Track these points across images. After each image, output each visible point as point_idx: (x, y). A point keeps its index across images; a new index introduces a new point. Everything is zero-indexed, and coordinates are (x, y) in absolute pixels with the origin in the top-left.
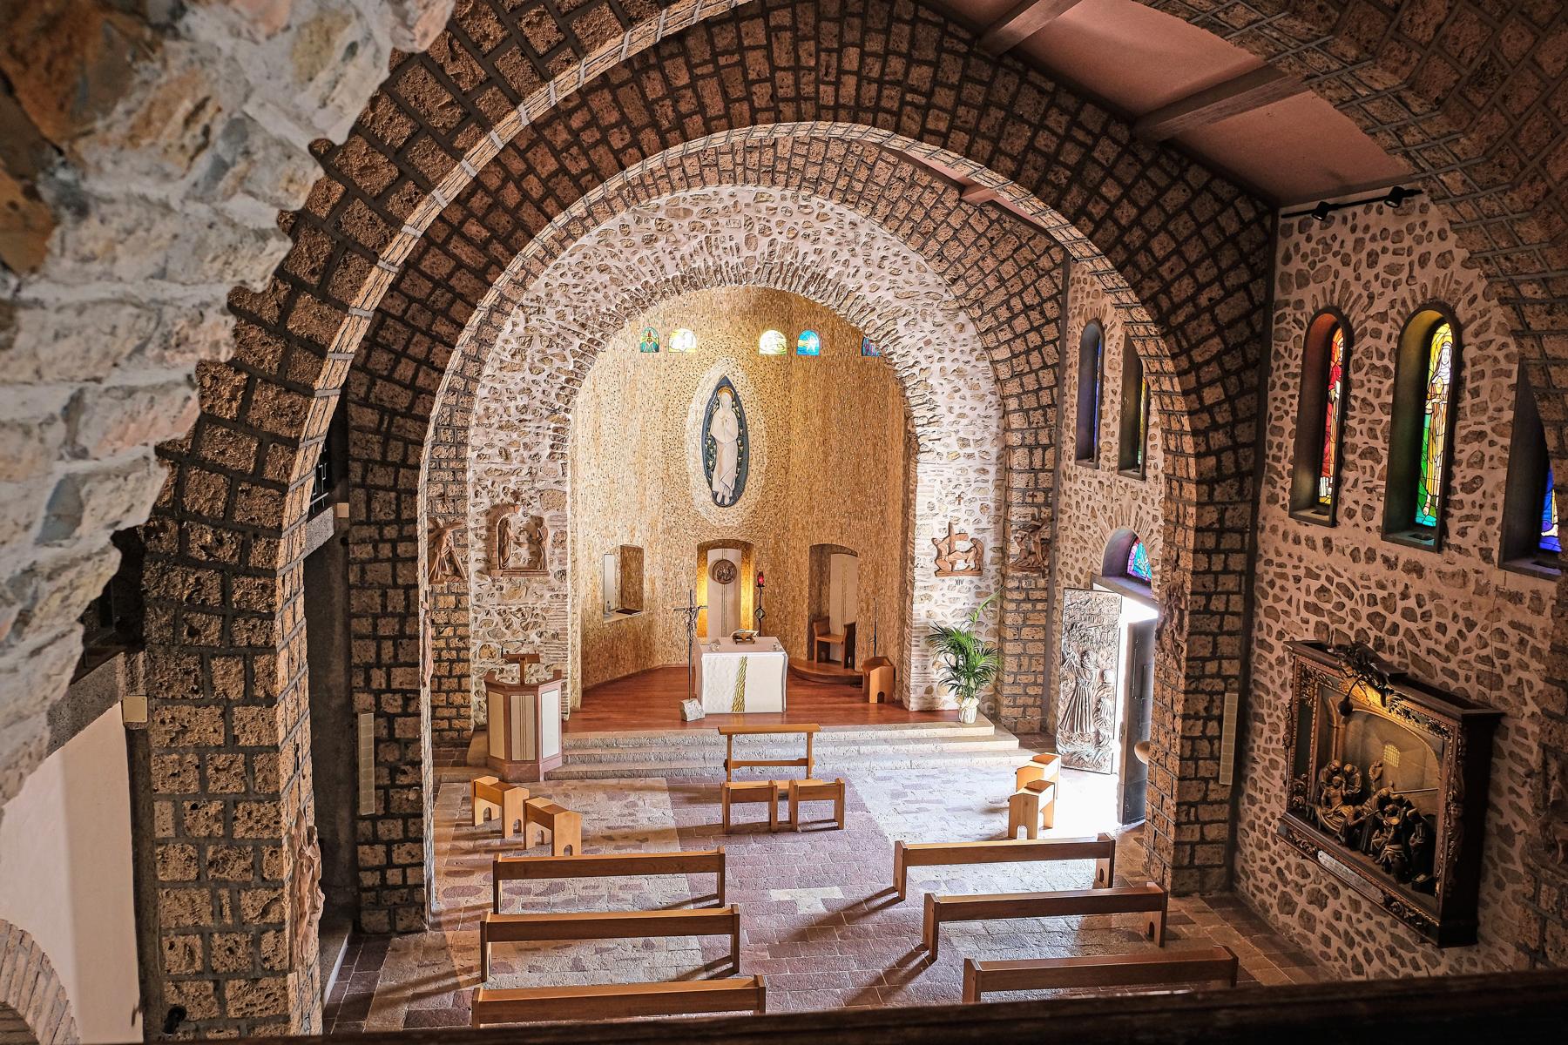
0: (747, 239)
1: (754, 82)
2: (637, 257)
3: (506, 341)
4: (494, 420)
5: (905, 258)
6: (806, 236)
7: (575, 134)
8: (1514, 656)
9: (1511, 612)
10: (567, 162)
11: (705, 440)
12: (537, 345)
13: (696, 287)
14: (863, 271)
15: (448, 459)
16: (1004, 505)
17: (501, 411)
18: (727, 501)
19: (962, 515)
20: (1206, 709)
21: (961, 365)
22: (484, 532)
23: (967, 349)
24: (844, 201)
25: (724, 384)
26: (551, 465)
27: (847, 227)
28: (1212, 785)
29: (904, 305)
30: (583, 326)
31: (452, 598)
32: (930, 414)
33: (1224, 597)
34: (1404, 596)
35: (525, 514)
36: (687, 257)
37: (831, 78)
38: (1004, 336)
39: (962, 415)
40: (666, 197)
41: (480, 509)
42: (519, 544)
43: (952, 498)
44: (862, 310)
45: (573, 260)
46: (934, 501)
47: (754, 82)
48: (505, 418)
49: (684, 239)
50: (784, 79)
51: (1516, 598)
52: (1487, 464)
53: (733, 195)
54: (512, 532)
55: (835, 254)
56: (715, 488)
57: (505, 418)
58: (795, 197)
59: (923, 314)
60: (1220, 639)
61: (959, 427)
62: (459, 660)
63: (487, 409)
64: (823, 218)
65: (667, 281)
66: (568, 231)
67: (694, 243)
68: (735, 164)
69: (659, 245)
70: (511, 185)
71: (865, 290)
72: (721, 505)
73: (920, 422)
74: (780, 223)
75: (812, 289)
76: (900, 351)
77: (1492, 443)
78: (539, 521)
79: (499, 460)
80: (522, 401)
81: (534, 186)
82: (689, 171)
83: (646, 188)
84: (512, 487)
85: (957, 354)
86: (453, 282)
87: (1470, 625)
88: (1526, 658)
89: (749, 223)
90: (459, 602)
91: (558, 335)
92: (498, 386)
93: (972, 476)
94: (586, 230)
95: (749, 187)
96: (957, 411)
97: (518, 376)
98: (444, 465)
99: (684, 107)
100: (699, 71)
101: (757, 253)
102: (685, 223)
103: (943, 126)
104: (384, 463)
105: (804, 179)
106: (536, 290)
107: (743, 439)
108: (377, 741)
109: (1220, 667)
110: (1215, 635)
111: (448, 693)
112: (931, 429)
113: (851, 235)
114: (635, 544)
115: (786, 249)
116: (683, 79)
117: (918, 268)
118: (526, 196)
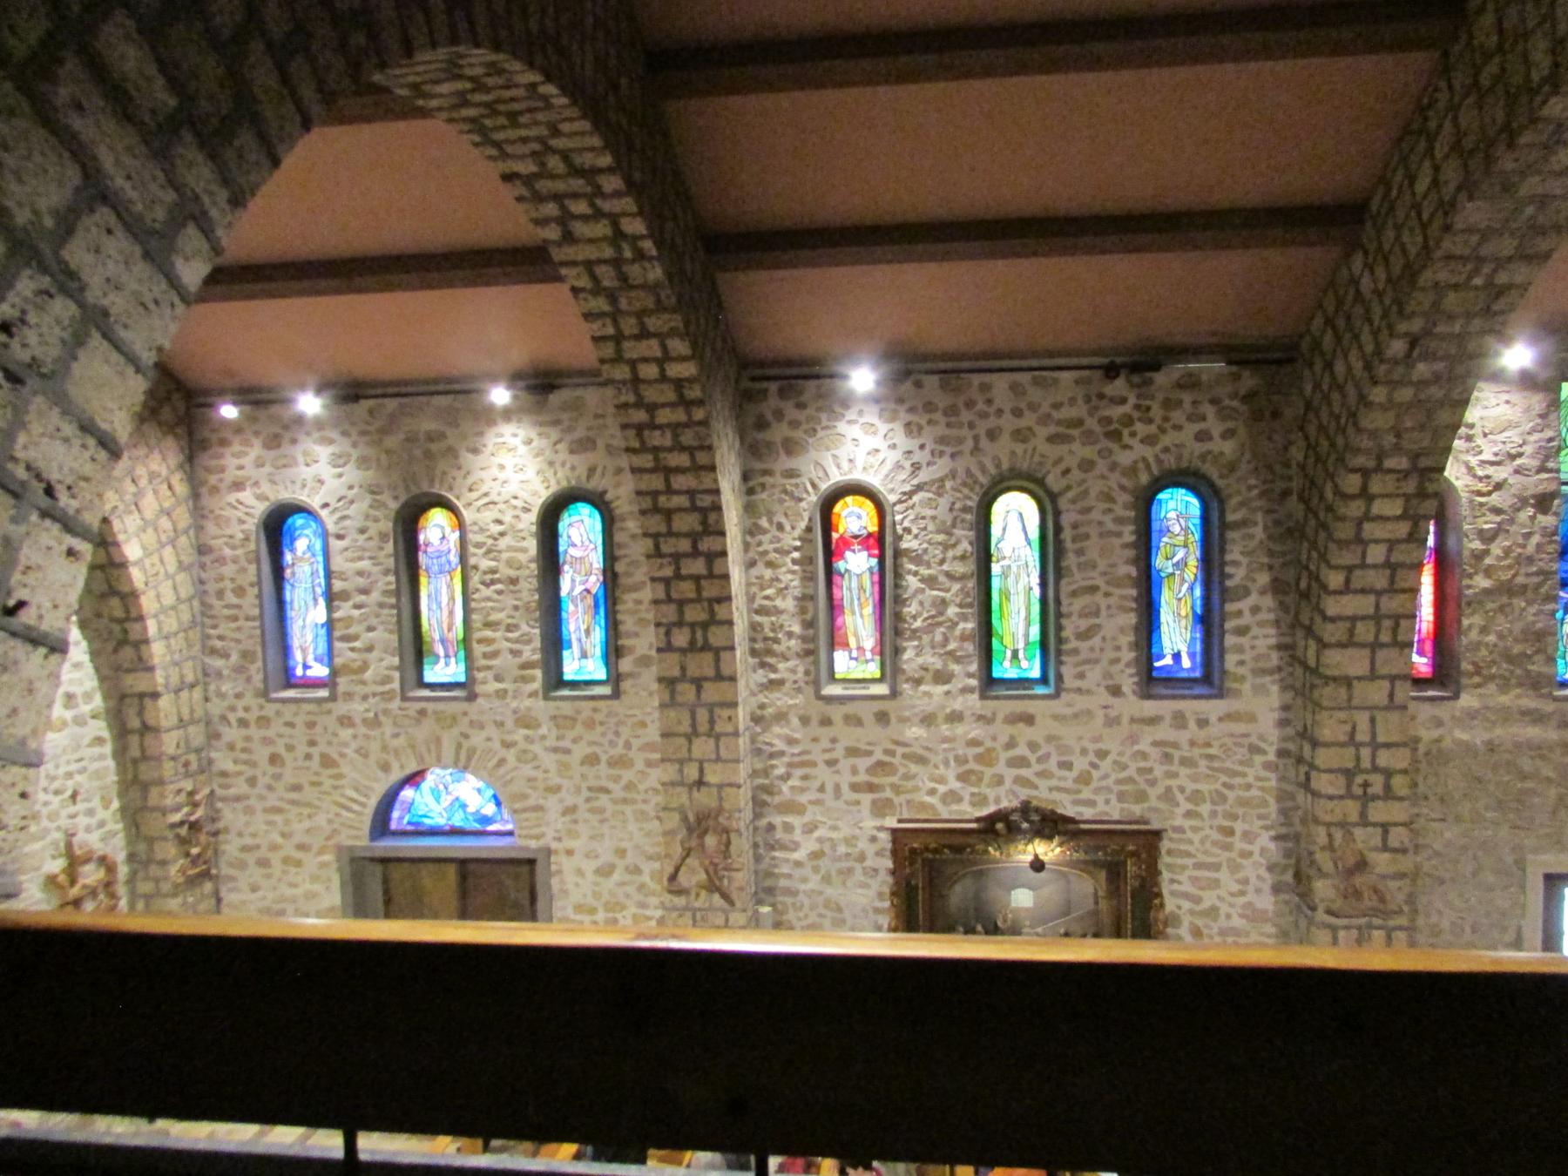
8: (1159, 771)
9: (1148, 736)
34: (1011, 744)
51: (1153, 721)
52: (1104, 613)
77: (1107, 595)
87: (1102, 754)
88: (1174, 768)
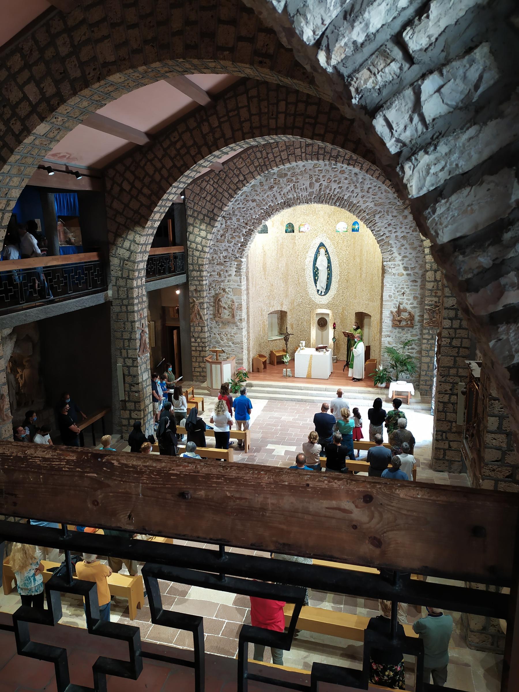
0: (310, 184)
1: (244, 122)
2: (266, 195)
3: (219, 231)
4: (215, 261)
5: (379, 187)
6: (335, 181)
7: (178, 151)
10: (176, 163)
12: (230, 232)
15: (197, 277)
16: (423, 296)
17: (218, 258)
18: (323, 294)
20: (451, 389)
21: (405, 234)
22: (212, 304)
23: (408, 227)
24: (348, 164)
25: (322, 245)
27: (353, 175)
28: (454, 424)
30: (246, 224)
31: (200, 328)
33: (460, 340)
36: (286, 193)
37: (274, 116)
40: (276, 169)
41: (212, 295)
44: (360, 212)
45: (242, 198)
46: (391, 294)
47: (244, 122)
48: (219, 260)
49: (285, 186)
50: (255, 119)
53: (304, 166)
55: (348, 188)
57: (219, 260)
58: (330, 164)
59: (388, 212)
60: (458, 359)
61: (404, 262)
62: (202, 351)
63: (213, 257)
64: (342, 172)
65: (278, 204)
66: (237, 186)
67: (289, 188)
68: (302, 153)
69: (274, 189)
70: (157, 173)
71: (361, 203)
72: (321, 295)
74: (324, 176)
75: (338, 204)
76: (377, 229)
79: (218, 277)
80: (225, 254)
81: (164, 172)
82: (283, 158)
83: (266, 166)
85: (403, 229)
86: (140, 211)
89: (311, 177)
90: (202, 329)
91: (237, 228)
92: (216, 248)
94: (244, 185)
95: (310, 161)
97: (223, 244)
98: (195, 278)
99: (217, 135)
100: (222, 120)
101: (314, 190)
102: (285, 179)
103: (322, 132)
104: (122, 278)
105: (331, 156)
106: (229, 210)
107: (329, 268)
108: (124, 375)
109: (458, 371)
110: (455, 357)
111: (199, 362)
113: (355, 179)
114: (283, 310)
115: (327, 187)
116: (216, 124)
117: (385, 191)
118: (162, 176)
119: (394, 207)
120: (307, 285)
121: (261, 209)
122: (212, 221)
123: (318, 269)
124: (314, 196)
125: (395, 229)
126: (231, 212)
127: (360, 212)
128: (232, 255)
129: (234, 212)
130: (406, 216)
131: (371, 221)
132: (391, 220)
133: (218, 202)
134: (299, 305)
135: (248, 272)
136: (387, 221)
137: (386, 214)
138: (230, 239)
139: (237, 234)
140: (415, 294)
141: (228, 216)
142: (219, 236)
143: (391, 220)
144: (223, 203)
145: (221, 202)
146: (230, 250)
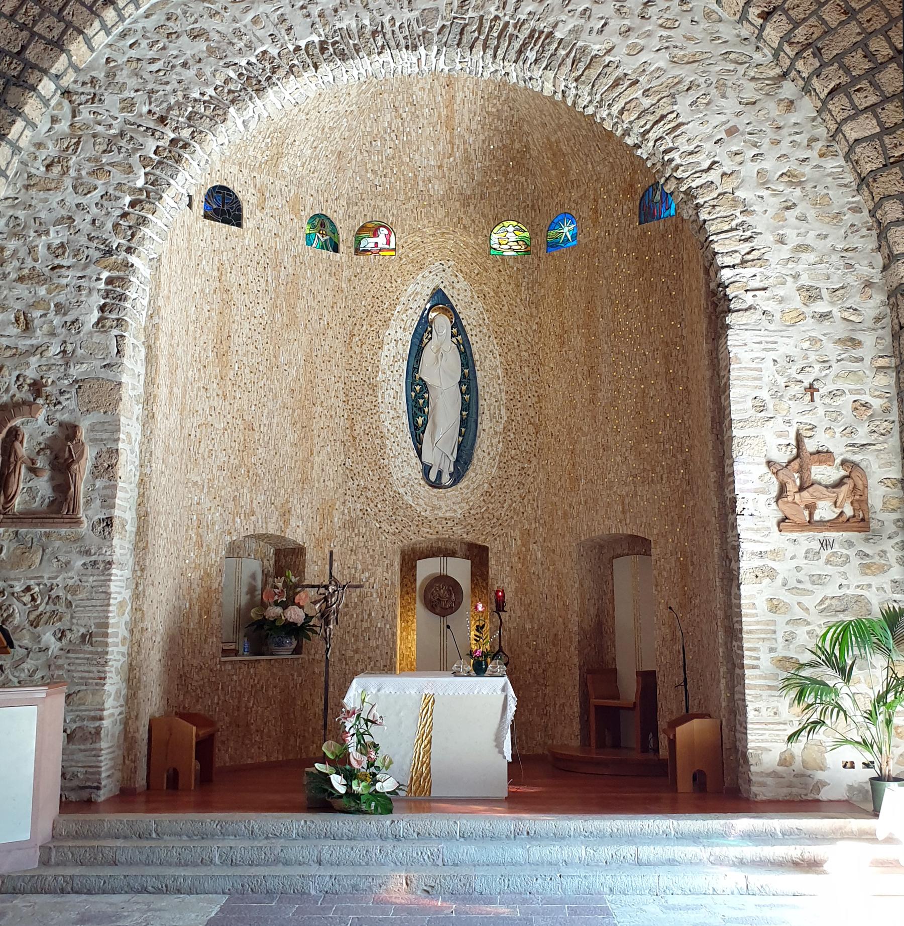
2: (251, 15)
3: (39, 145)
11: (410, 386)
12: (88, 150)
13: (343, 56)
14: (615, 24)
17: (22, 253)
19: (818, 416)
23: (802, 139)
26: (97, 338)
29: (687, 74)
30: (162, 120)
32: (745, 247)
35: (49, 421)
38: (862, 100)
39: (802, 248)
42: (33, 470)
43: (796, 389)
44: (616, 83)
45: (150, 23)
46: (765, 394)
54: (23, 449)
56: (427, 457)
57: (29, 263)
59: (721, 87)
61: (800, 267)
65: (298, 49)
72: (436, 485)
73: (728, 261)
75: (531, 55)
78: (70, 431)
79: (14, 330)
80: (55, 237)
84: (31, 374)
91: (122, 134)
92: (21, 214)
93: (832, 351)
96: (793, 239)
97: (55, 198)
106: (90, 67)
112: (748, 272)
119: (741, 69)
120: (383, 447)
121: (227, 65)
122: (13, 90)
123: (425, 386)
124: (438, 25)
125: (755, 145)
126: (101, 75)
127: (616, 83)
128: (90, 239)
129: (111, 75)
130: (792, 102)
131: (663, 117)
132: (738, 114)
133: (50, 20)
134: (350, 525)
135: (156, 326)
136: (723, 118)
137: (713, 91)
138: (86, 179)
139: (119, 158)
140: (858, 391)
141: (88, 89)
142: (38, 163)
143: (738, 114)
144: (69, 25)
145: (61, 19)
146: (83, 222)
